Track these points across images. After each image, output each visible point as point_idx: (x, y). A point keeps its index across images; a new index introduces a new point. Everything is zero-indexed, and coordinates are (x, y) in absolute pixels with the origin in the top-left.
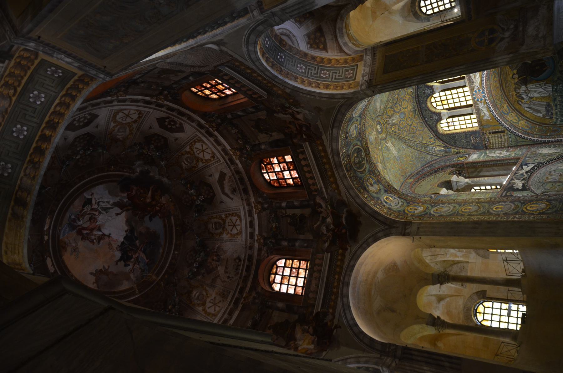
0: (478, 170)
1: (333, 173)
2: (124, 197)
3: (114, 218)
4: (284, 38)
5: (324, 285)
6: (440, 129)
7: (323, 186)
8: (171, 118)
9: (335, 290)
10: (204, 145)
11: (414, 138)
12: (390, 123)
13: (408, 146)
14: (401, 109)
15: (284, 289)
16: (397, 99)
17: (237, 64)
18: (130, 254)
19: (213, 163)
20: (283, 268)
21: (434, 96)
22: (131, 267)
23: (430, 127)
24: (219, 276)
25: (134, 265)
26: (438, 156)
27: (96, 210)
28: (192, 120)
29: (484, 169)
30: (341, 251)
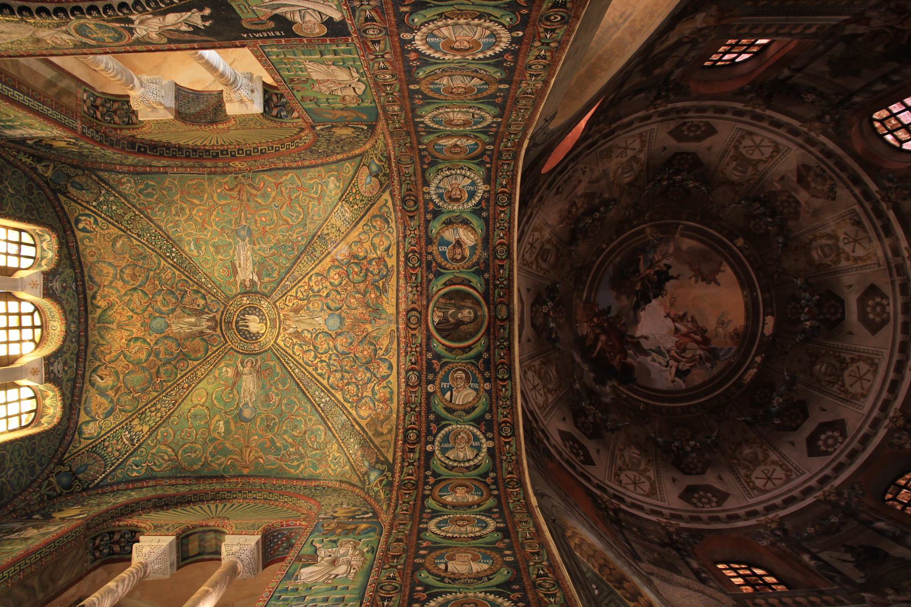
0: (55, 90)
6: (45, 245)
11: (141, 254)
12: (208, 320)
13: (174, 243)
14: (156, 344)
16: (158, 372)
18: (655, 277)
21: (32, 345)
22: (665, 261)
23: (72, 260)
24: (589, 182)
25: (659, 261)
26: (97, 176)
27: (672, 357)
28: (554, 447)
29: (39, 85)
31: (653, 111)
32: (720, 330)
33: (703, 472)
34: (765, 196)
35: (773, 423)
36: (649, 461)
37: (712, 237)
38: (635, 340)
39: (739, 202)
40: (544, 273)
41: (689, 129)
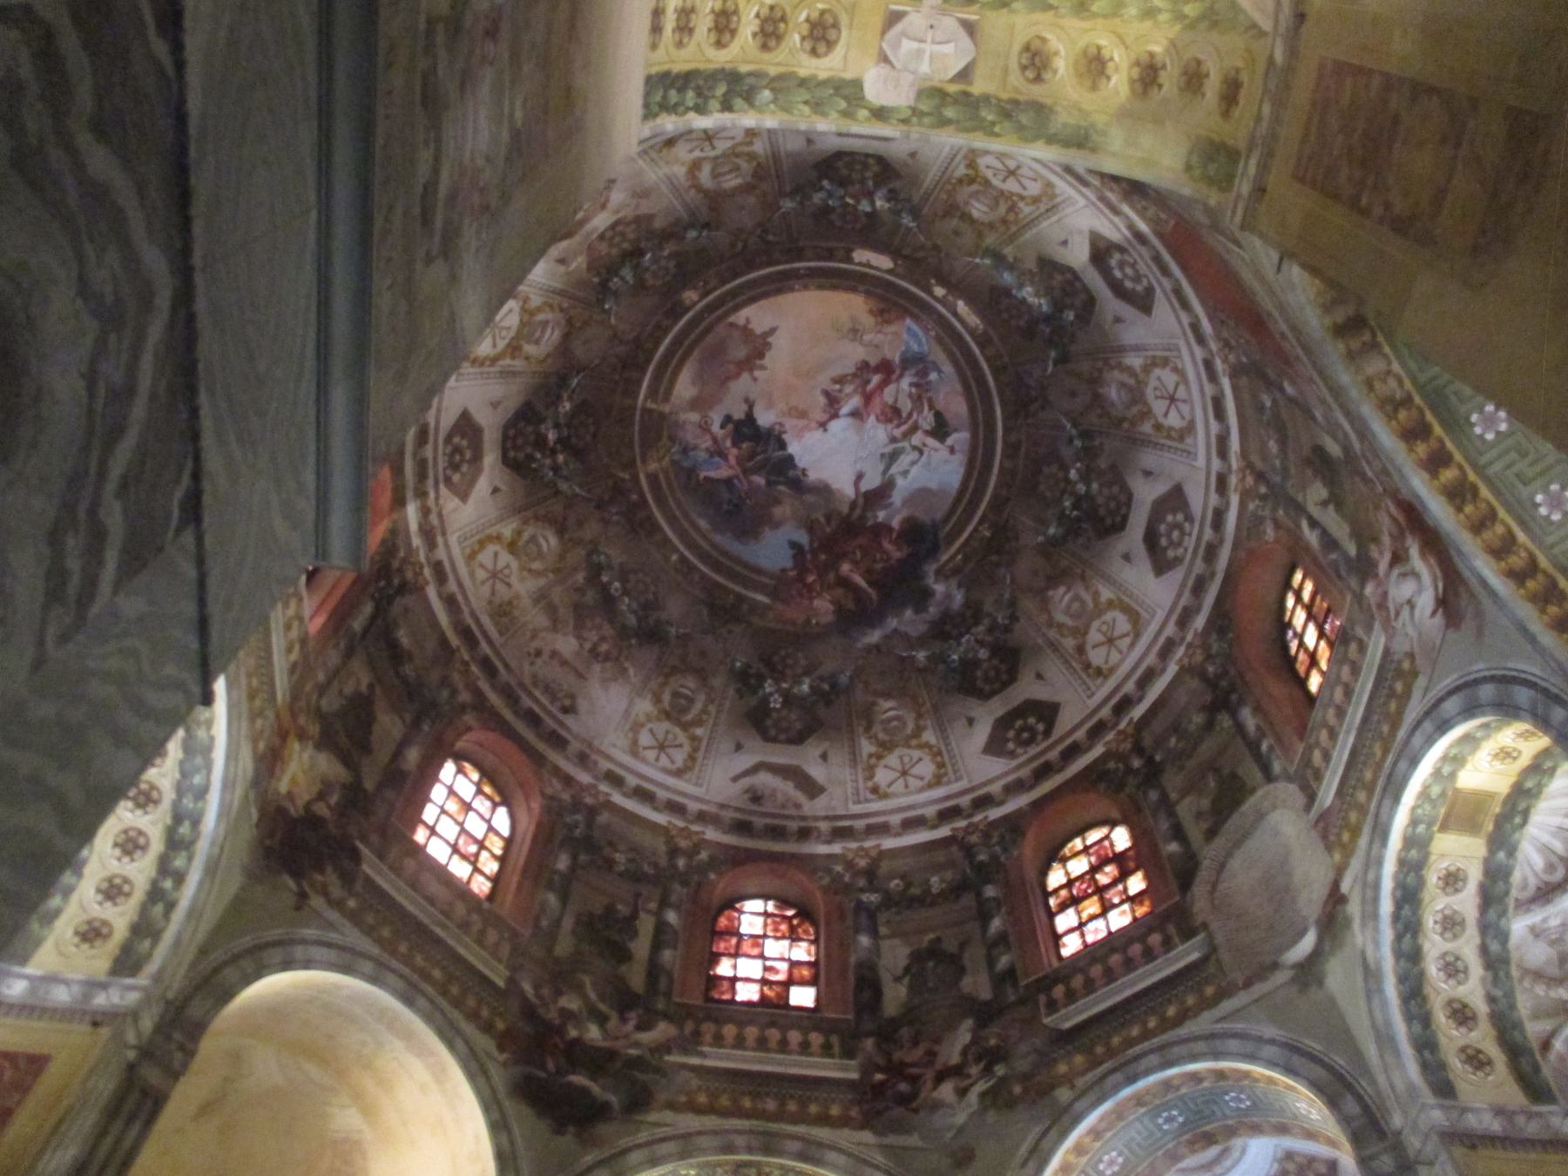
1: (747, 1115)
2: (893, 515)
3: (855, 462)
4: (1213, 1151)
5: (426, 920)
7: (709, 1063)
8: (1043, 740)
9: (403, 948)
10: (919, 783)
15: (438, 793)
17: (1210, 991)
18: (745, 446)
19: (856, 781)
20: (487, 816)
22: (716, 428)
24: (555, 629)
25: (715, 440)
27: (907, 435)
30: (500, 1025)
31: (427, 572)
32: (867, 337)
33: (1130, 496)
34: (599, 274)
35: (1072, 323)
36: (1083, 578)
37: (677, 342)
38: (861, 501)
39: (604, 311)
40: (712, 701)
41: (455, 467)
